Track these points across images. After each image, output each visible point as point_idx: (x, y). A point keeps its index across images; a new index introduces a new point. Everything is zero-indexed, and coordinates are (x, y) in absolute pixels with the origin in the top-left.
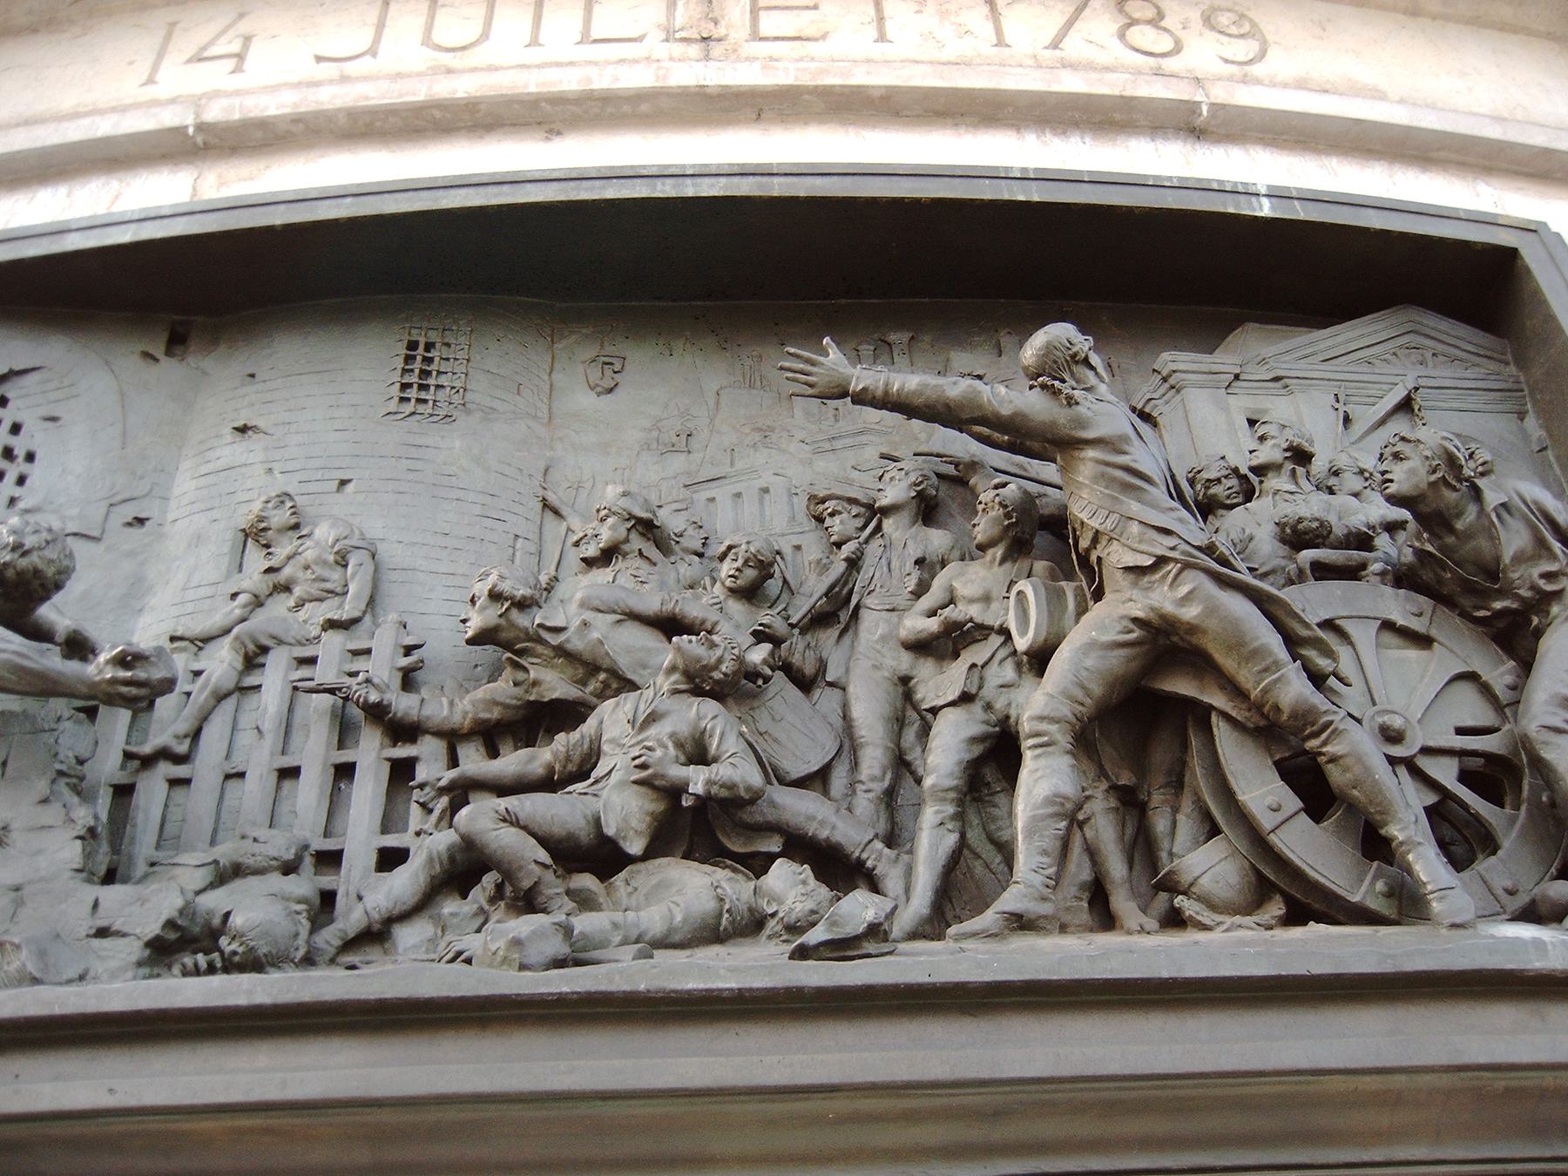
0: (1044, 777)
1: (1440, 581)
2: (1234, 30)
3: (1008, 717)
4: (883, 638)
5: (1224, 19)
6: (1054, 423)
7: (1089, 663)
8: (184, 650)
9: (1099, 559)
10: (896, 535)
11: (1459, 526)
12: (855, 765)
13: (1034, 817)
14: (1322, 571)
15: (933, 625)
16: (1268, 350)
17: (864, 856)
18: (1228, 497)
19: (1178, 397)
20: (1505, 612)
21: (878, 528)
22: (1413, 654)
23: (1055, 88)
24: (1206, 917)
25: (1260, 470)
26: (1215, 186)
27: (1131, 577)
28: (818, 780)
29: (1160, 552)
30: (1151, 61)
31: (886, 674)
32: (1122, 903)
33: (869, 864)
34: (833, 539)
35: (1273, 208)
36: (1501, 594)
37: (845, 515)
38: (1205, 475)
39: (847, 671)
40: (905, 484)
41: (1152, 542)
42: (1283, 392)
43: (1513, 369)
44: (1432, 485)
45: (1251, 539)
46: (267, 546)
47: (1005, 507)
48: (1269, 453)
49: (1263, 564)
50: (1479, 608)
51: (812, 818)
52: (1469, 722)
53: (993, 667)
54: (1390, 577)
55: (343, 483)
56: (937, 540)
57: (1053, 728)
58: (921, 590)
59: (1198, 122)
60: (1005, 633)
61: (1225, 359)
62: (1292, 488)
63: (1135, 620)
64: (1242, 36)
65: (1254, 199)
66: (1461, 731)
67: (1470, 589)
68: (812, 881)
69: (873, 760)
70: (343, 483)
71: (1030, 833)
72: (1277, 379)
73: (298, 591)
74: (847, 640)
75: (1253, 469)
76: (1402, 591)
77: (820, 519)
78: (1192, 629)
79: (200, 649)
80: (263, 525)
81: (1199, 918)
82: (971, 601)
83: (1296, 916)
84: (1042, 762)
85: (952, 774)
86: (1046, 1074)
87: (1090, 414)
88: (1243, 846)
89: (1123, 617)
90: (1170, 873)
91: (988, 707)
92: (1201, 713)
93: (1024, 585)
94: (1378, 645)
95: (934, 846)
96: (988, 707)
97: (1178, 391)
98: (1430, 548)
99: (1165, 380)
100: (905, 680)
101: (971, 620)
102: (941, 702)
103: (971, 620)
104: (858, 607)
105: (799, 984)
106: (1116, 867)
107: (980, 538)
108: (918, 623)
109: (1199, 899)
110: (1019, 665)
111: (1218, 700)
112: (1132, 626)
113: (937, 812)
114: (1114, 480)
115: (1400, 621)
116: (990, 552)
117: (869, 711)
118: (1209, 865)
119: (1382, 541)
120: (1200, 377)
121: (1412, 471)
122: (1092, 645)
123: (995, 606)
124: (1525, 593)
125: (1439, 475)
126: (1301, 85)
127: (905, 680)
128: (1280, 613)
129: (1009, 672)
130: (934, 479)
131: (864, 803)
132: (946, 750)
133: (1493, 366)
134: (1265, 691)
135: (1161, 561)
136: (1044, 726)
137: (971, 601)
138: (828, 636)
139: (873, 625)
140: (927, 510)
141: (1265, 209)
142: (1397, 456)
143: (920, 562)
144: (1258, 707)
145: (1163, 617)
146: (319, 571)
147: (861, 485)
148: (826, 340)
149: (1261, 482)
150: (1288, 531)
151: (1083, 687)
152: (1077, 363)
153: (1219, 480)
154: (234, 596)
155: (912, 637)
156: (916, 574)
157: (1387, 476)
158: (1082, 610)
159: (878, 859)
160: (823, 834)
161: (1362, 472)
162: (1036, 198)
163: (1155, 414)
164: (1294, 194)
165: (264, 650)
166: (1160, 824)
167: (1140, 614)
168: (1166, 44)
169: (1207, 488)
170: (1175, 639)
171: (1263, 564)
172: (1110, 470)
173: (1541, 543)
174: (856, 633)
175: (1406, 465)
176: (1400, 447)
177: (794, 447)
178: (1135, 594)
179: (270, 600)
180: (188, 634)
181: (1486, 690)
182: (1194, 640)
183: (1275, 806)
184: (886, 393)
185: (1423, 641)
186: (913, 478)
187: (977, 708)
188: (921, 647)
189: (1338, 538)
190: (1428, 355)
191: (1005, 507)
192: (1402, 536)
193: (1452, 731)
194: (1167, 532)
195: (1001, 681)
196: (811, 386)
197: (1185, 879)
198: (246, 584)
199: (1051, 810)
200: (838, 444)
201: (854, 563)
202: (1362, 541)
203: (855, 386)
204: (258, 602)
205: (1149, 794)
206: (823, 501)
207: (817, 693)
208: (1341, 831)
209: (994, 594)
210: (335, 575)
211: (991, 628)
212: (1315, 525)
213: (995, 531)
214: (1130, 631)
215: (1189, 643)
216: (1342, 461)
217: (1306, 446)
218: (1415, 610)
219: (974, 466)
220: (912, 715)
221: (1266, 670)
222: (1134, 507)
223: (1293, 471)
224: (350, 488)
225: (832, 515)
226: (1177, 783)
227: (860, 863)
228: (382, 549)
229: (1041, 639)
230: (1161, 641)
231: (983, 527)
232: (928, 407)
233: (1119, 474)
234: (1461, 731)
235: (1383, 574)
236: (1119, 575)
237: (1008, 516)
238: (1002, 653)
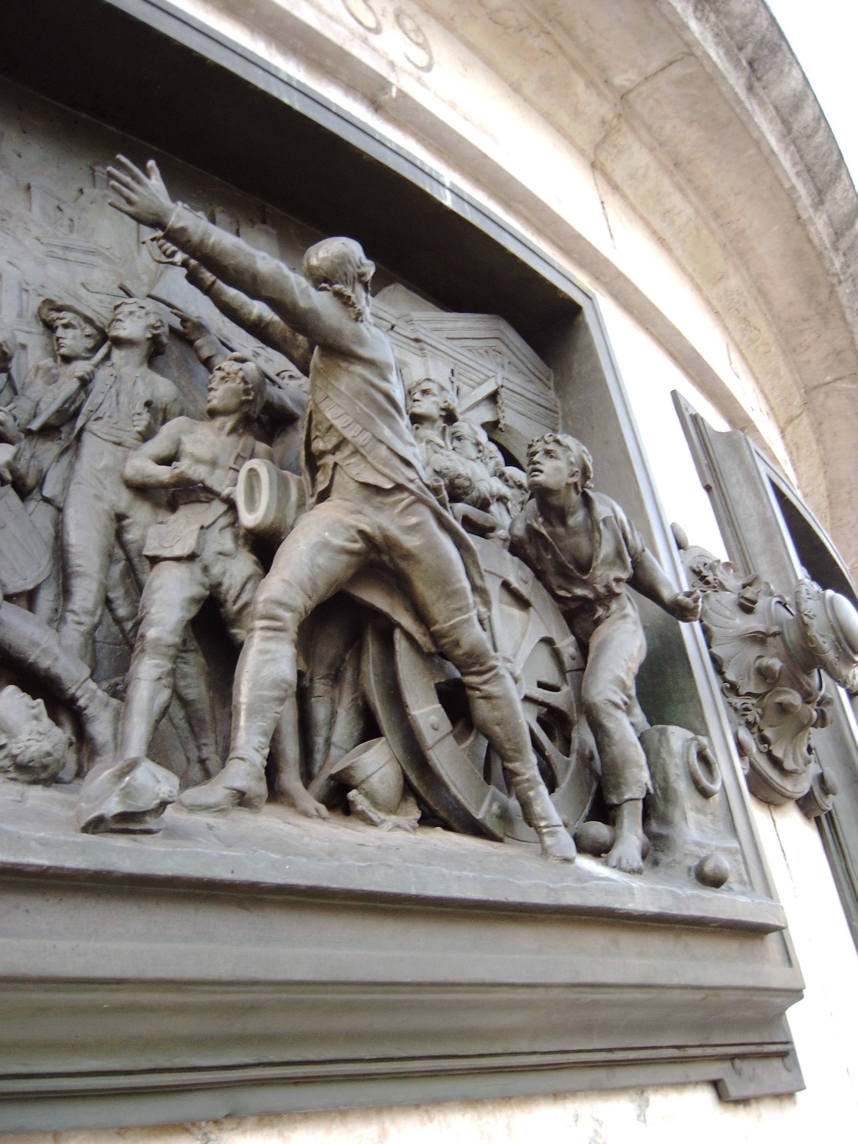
0: (267, 662)
1: (539, 558)
2: (413, 35)
3: (220, 584)
4: (106, 469)
5: (409, 24)
6: (339, 332)
7: (321, 560)
9: (336, 464)
10: (125, 370)
11: (571, 521)
12: (65, 592)
13: (260, 698)
15: (164, 473)
16: (416, 315)
17: (79, 693)
20: (584, 599)
21: (107, 357)
22: (516, 612)
23: (296, 13)
24: (374, 814)
26: (419, 164)
27: (366, 492)
28: (29, 599)
29: (401, 480)
30: (361, 30)
31: (107, 507)
32: (291, 779)
33: (82, 702)
34: (63, 351)
35: (452, 201)
36: (585, 584)
37: (78, 332)
39: (65, 489)
40: (143, 323)
41: (393, 469)
42: (419, 352)
43: (552, 394)
44: (568, 485)
47: (246, 383)
50: (561, 588)
51: (36, 644)
52: (545, 679)
53: (214, 533)
54: (508, 544)
56: (163, 388)
57: (288, 615)
58: (147, 435)
59: (383, 98)
60: (231, 506)
62: (441, 442)
63: (361, 532)
64: (418, 44)
65: (441, 188)
66: (541, 685)
67: (563, 572)
68: (46, 721)
69: (85, 593)
71: (253, 712)
72: (417, 340)
74: (66, 459)
77: (50, 327)
78: (408, 556)
81: (371, 814)
82: (199, 461)
83: (429, 819)
84: (272, 646)
85: (175, 630)
86: (309, 977)
87: (368, 335)
88: (399, 752)
89: (352, 526)
90: (349, 768)
91: (206, 569)
92: (386, 629)
93: (254, 463)
95: (152, 699)
96: (206, 569)
100: (120, 517)
101: (202, 482)
102: (166, 553)
103: (202, 482)
104: (82, 430)
105: (111, 868)
106: (291, 749)
107: (215, 403)
108: (143, 464)
109: (367, 795)
110: (236, 537)
111: (405, 620)
112: (357, 537)
113: (157, 666)
114: (374, 401)
116: (219, 421)
117: (86, 540)
118: (377, 765)
121: (558, 470)
122: (325, 545)
123: (219, 472)
124: (601, 589)
126: (453, 106)
127: (120, 517)
129: (227, 542)
130: (166, 329)
131: (73, 634)
132: (168, 602)
133: (541, 387)
134: (454, 627)
135: (399, 488)
136: (280, 612)
137: (199, 461)
138: (49, 450)
139: (95, 453)
140: (155, 352)
141: (448, 201)
143: (148, 404)
144: (435, 637)
145: (386, 538)
147: (97, 306)
148: (151, 163)
151: (314, 583)
152: (360, 282)
155: (139, 479)
156: (146, 416)
158: (301, 506)
159: (90, 699)
160: (45, 663)
162: (297, 107)
164: (466, 198)
166: (320, 712)
167: (367, 529)
168: (370, 22)
170: (385, 558)
172: (373, 391)
173: (619, 554)
174: (77, 454)
177: (29, 241)
178: (367, 509)
181: (556, 654)
182: (403, 564)
183: (436, 726)
184: (202, 242)
185: (523, 603)
186: (152, 320)
187: (197, 567)
188: (141, 490)
190: (506, 361)
191: (246, 383)
193: (536, 684)
194: (408, 464)
195: (219, 548)
196: (129, 202)
197: (359, 775)
199: (276, 694)
200: (72, 256)
201: (85, 383)
203: (173, 221)
205: (311, 680)
206: (60, 309)
207: (32, 505)
208: (472, 753)
209: (221, 461)
211: (217, 495)
213: (233, 402)
214: (355, 541)
215: (395, 564)
219: (200, 328)
220: (119, 552)
221: (459, 609)
222: (387, 433)
223: (444, 429)
225: (66, 326)
226: (336, 678)
227: (74, 700)
229: (269, 521)
230: (373, 556)
231: (220, 394)
232: (236, 271)
233: (380, 398)
234: (541, 685)
235: (505, 540)
236: (353, 486)
237: (246, 392)
238: (224, 521)
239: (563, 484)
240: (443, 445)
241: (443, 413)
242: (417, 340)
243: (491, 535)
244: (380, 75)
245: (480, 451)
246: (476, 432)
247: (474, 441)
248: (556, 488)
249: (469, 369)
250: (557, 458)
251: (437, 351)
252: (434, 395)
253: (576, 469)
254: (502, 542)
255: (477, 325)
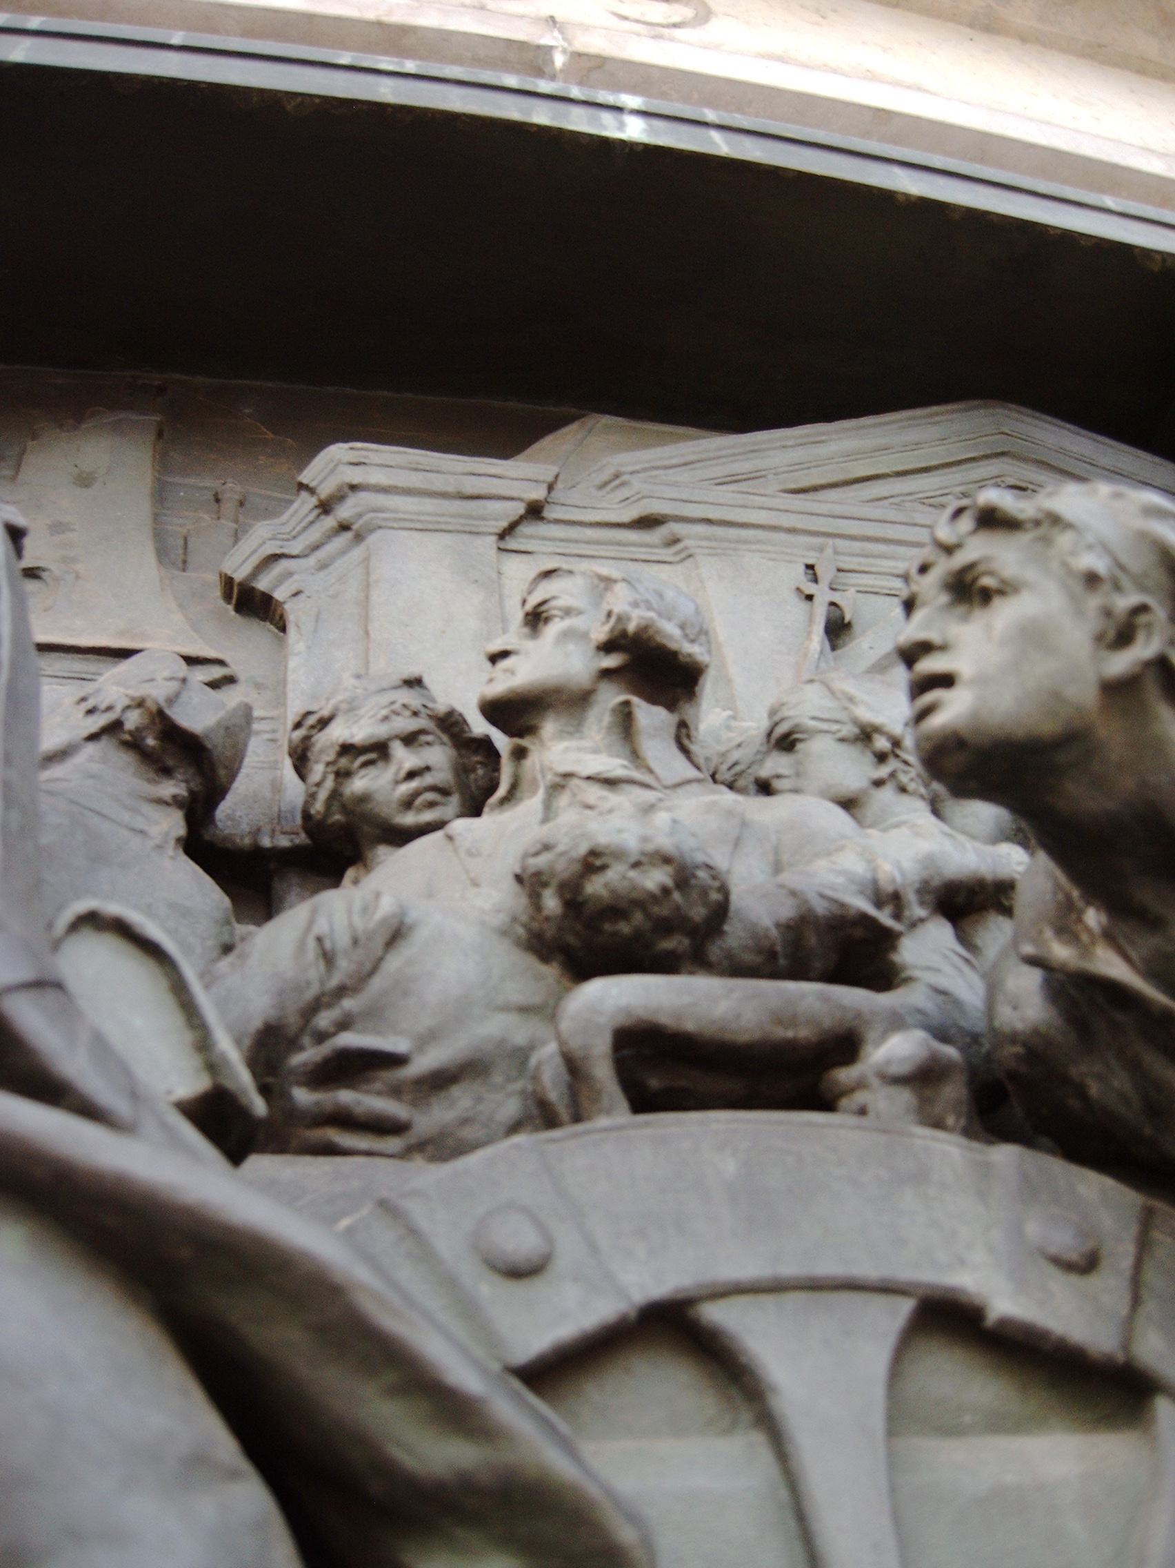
14: (665, 1071)
18: (408, 803)
19: (358, 553)
25: (517, 713)
38: (338, 732)
42: (665, 554)
44: (1119, 691)
45: (396, 934)
48: (540, 663)
49: (427, 1039)
54: (954, 1091)
61: (515, 477)
62: (614, 765)
72: (647, 522)
75: (496, 710)
76: (1005, 1155)
94: (901, 1416)
97: (359, 538)
98: (1111, 966)
99: (325, 507)
115: (1004, 1302)
119: (928, 949)
120: (429, 505)
121: (1033, 637)
125: (1143, 650)
128: (281, 1340)
142: (968, 590)
149: (520, 754)
150: (551, 903)
153: (379, 750)
157: (930, 665)
161: (866, 735)
163: (279, 595)
169: (343, 775)
171: (427, 1039)
175: (1004, 614)
176: (980, 549)
189: (756, 935)
192: (996, 933)
202: (854, 948)
212: (655, 879)
216: (809, 705)
217: (671, 633)
218: (1065, 1241)
235: (924, 1078)
239: (1085, 694)
240: (619, 773)
241: (612, 661)
242: (647, 522)
243: (845, 1075)
244: (509, 42)
245: (881, 758)
246: (851, 699)
247: (849, 730)
248: (1048, 727)
249: (882, 548)
250: (1006, 589)
251: (733, 532)
252: (568, 612)
253: (1124, 602)
254: (905, 1097)
255: (913, 435)
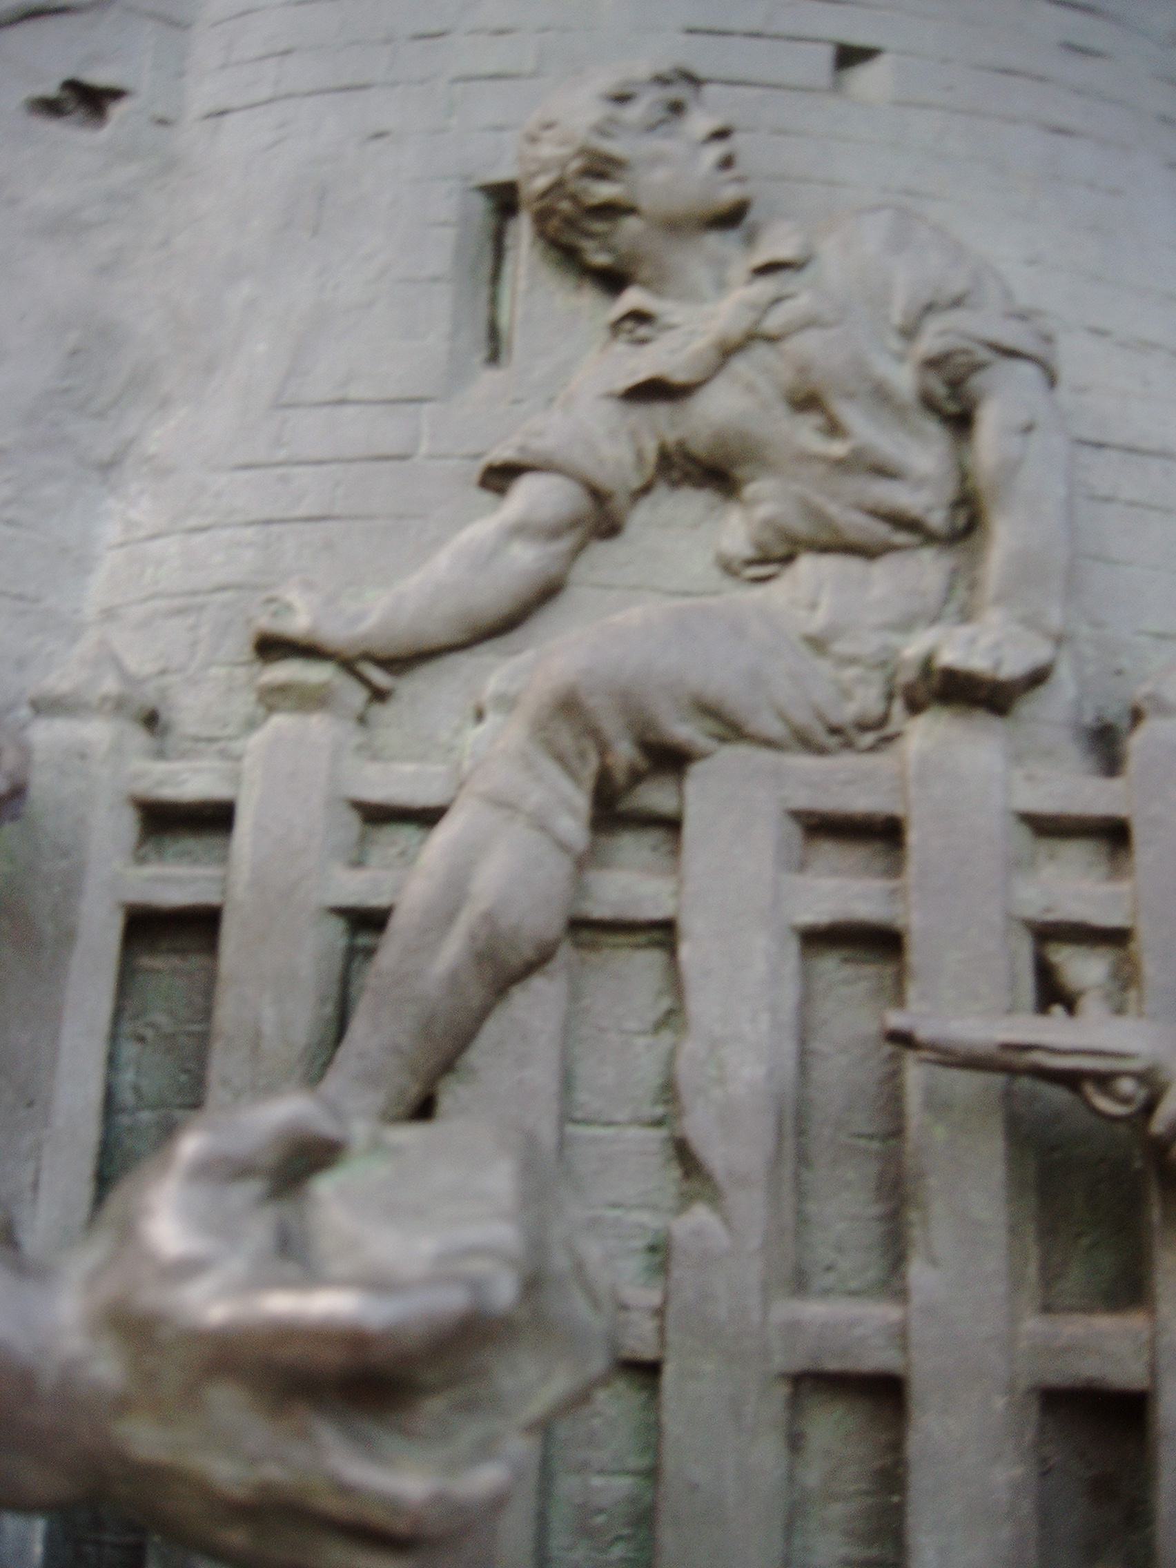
8: (310, 700)
46: (613, 281)
55: (850, 57)
70: (850, 57)
73: (767, 501)
79: (379, 695)
80: (604, 191)
146: (867, 430)
154: (499, 477)
165: (670, 760)
179: (645, 505)
180: (336, 631)
198: (545, 431)
204: (602, 518)
210: (924, 455)
224: (865, 78)
228: (1072, 354)
